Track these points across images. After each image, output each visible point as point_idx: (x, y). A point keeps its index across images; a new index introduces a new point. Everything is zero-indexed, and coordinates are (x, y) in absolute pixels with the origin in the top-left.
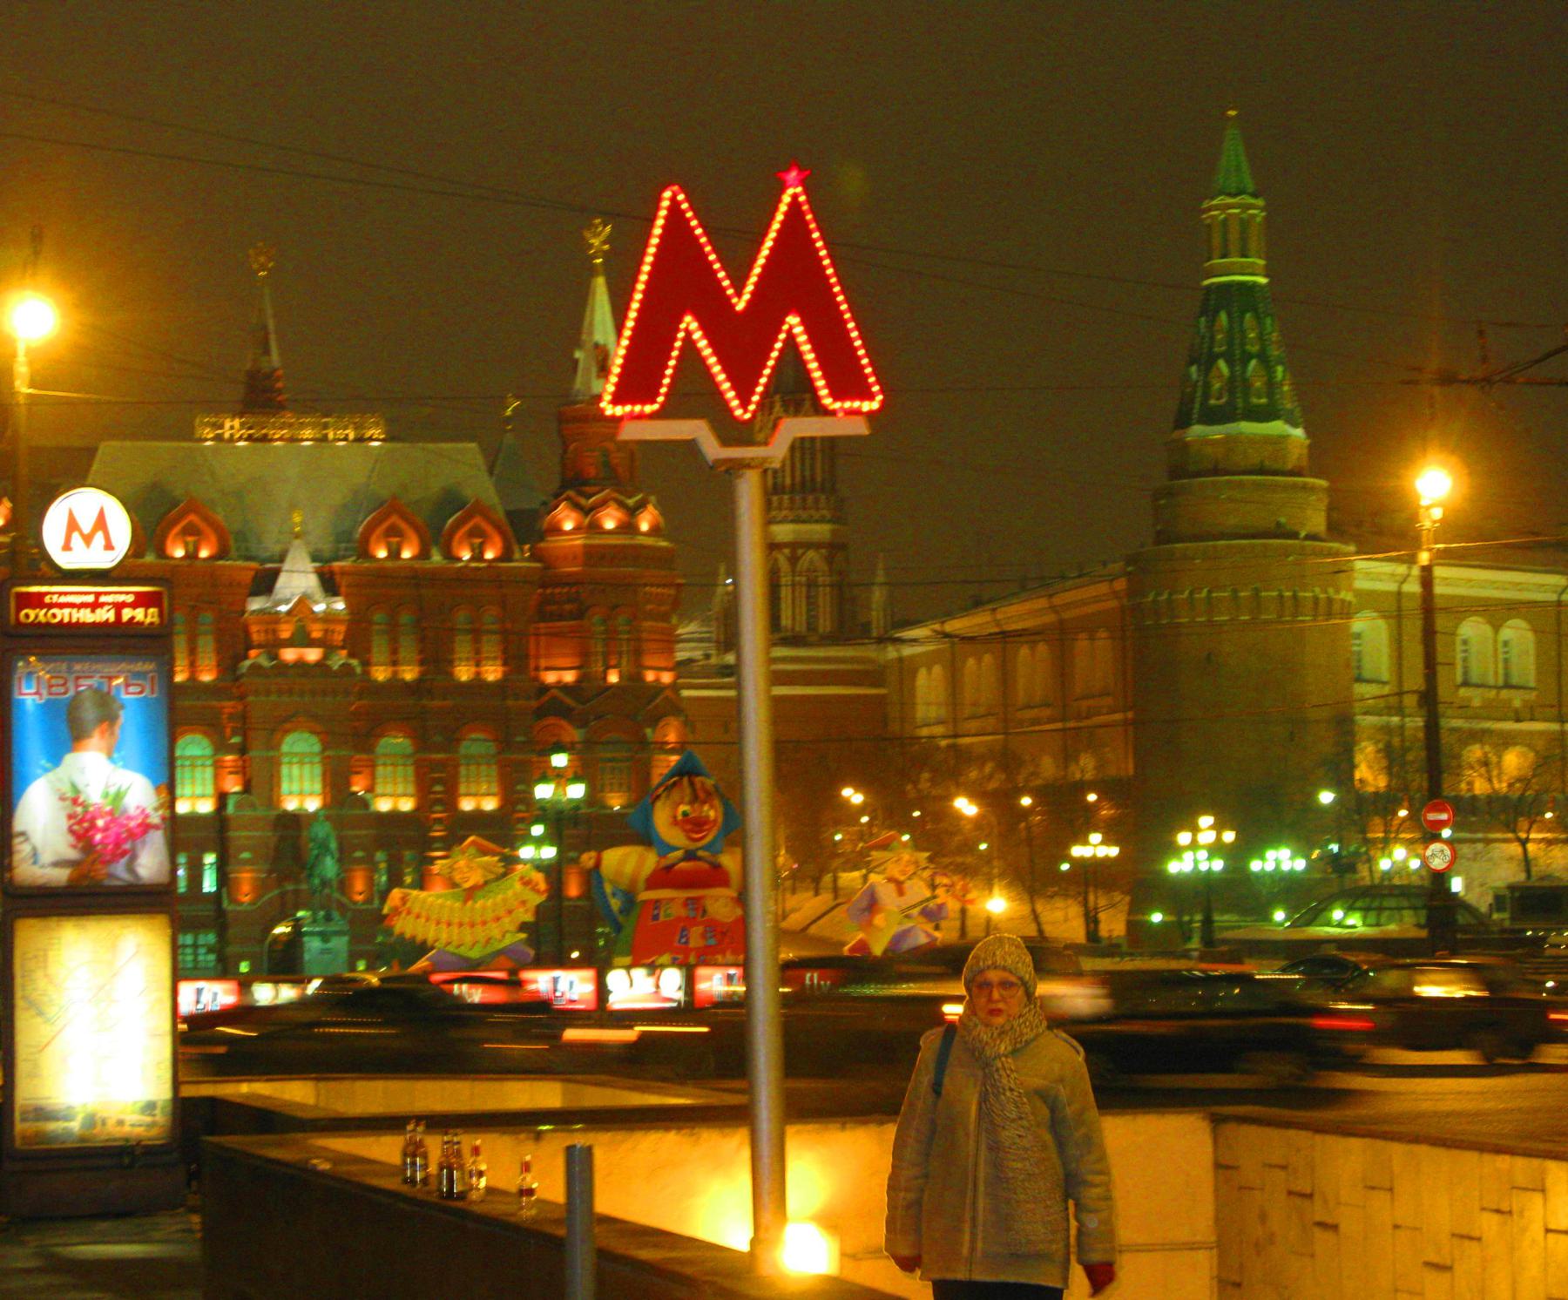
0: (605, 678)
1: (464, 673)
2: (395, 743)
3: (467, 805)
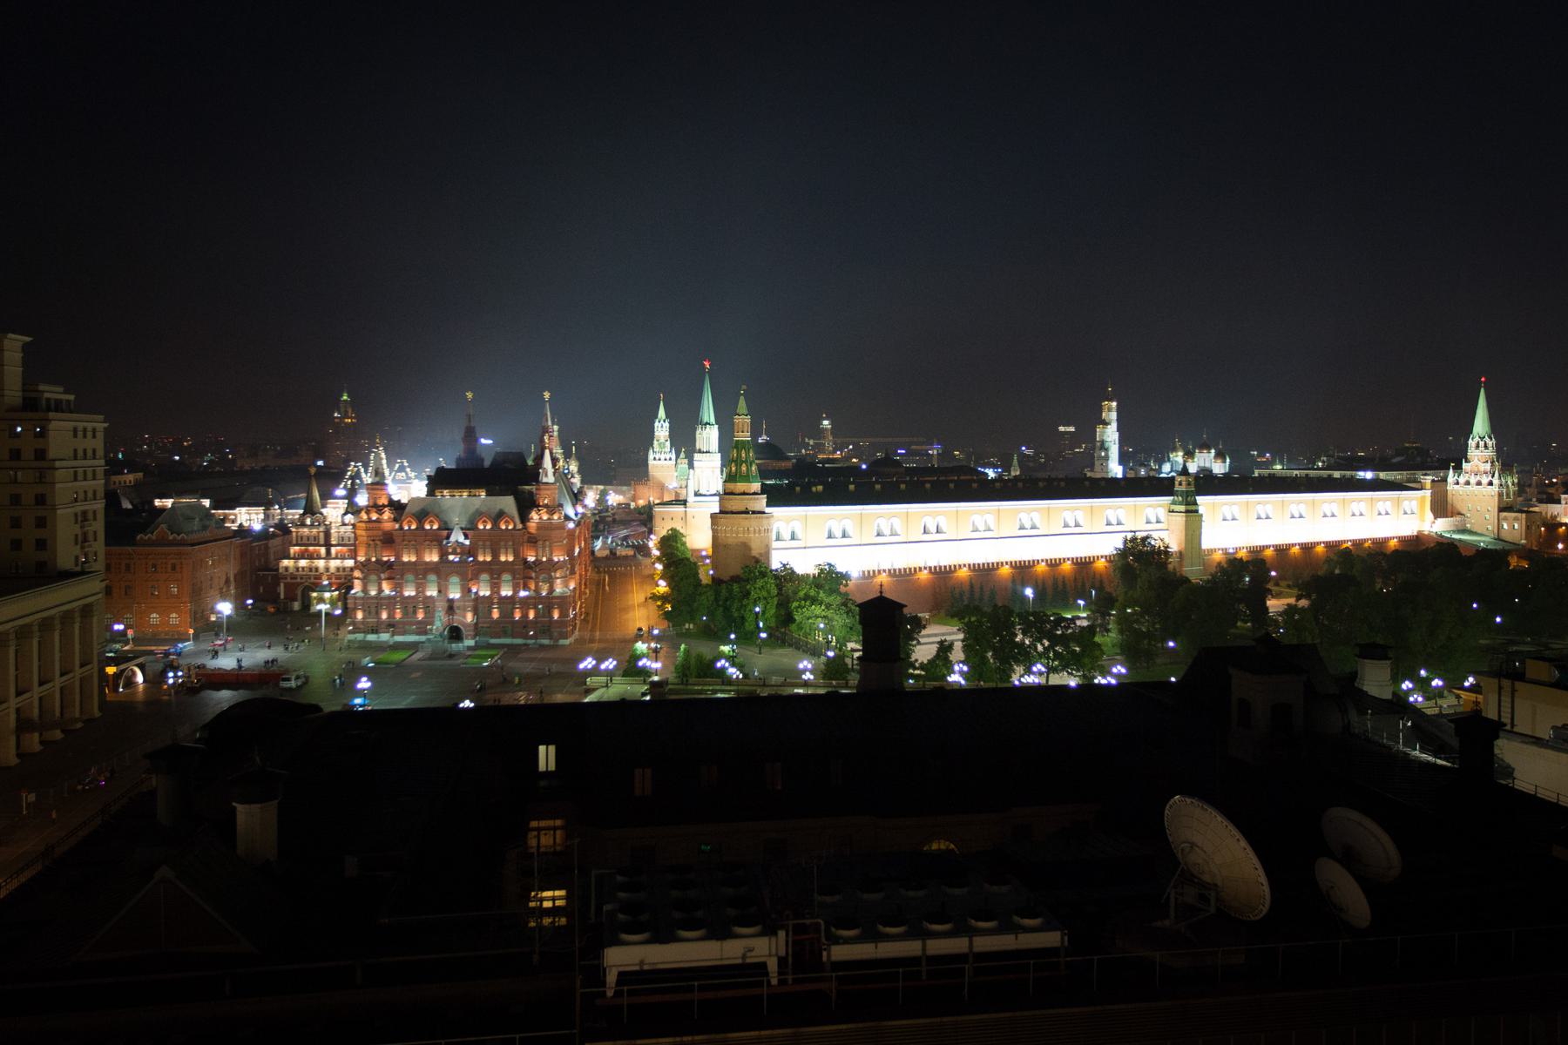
1: (503, 559)
3: (503, 593)
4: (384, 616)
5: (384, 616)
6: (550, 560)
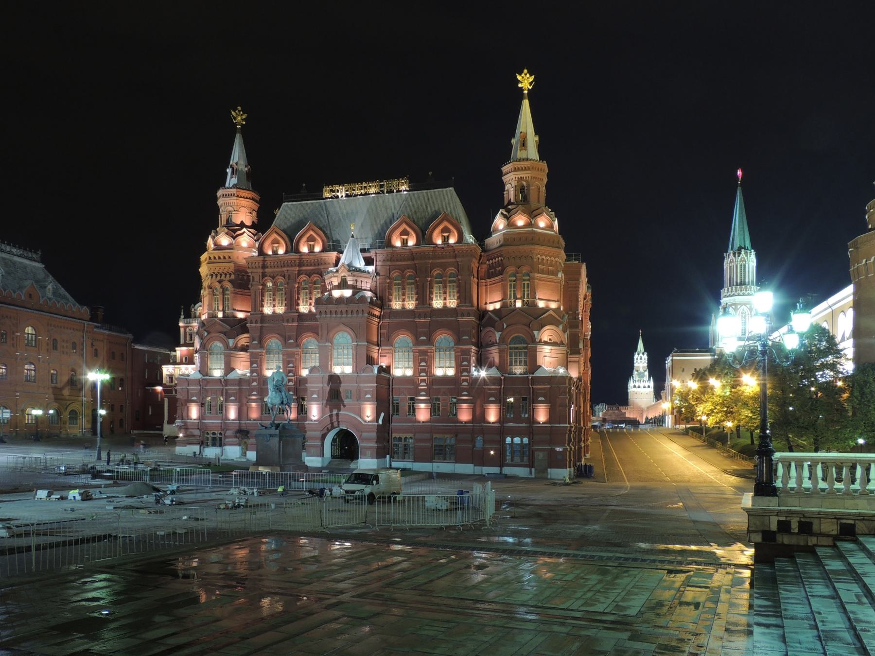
1: (437, 303)
3: (439, 372)
4: (232, 414)
5: (232, 414)
6: (530, 306)
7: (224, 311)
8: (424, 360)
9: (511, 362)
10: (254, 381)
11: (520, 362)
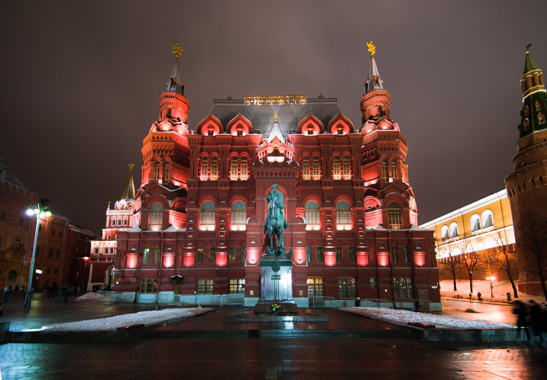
0: (388, 181)
2: (312, 202)
3: (340, 228)
4: (169, 262)
5: (169, 262)
7: (163, 179)
8: (330, 218)
9: (390, 221)
10: (190, 234)
11: (397, 221)
